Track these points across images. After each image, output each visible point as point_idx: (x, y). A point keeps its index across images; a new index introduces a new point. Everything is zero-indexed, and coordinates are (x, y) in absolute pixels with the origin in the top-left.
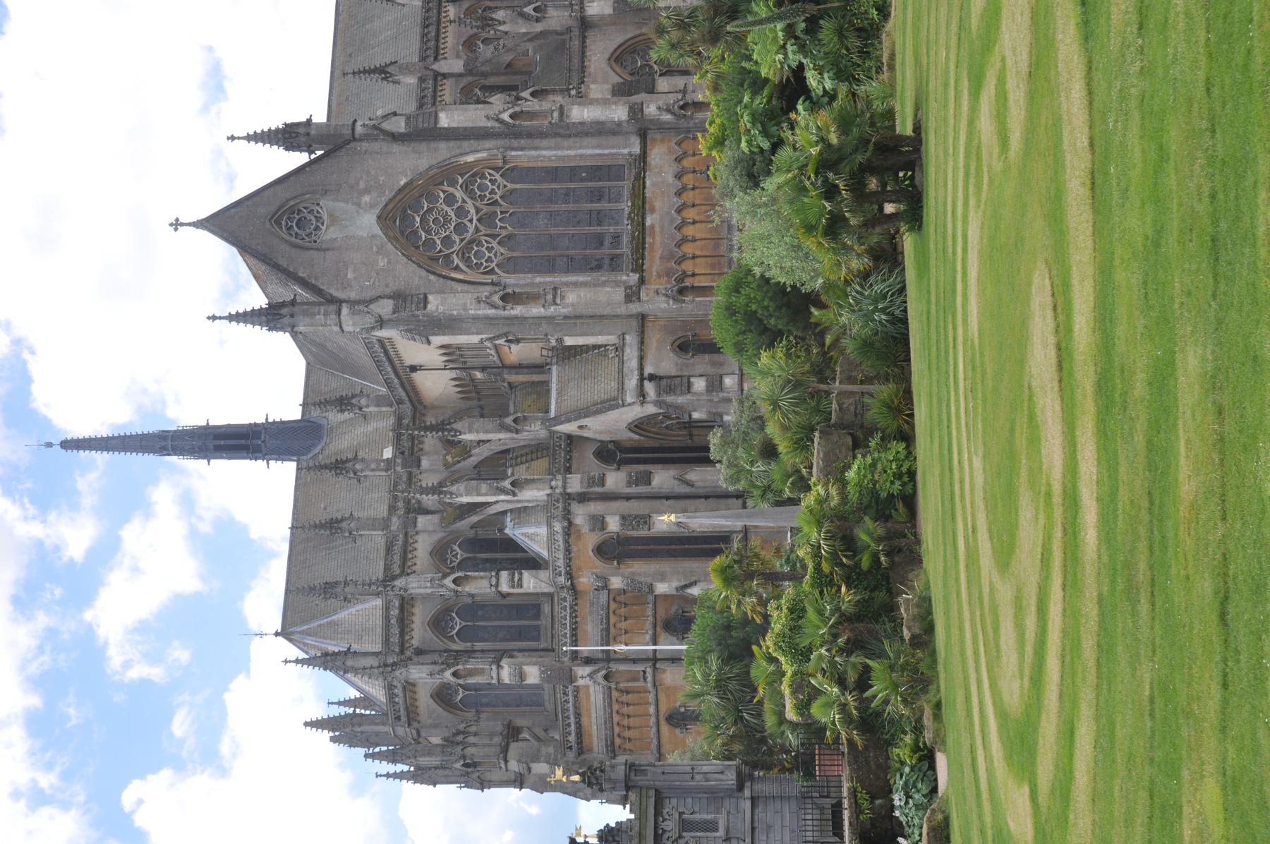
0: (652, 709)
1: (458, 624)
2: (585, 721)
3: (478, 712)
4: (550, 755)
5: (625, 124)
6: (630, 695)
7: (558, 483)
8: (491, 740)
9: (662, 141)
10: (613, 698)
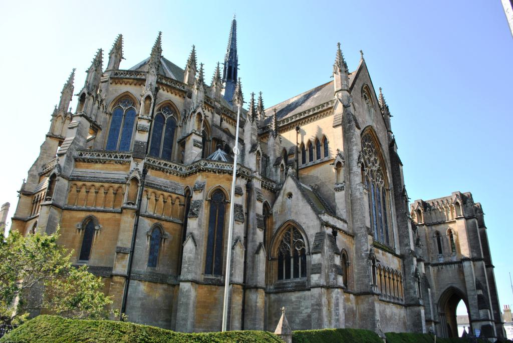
0: (99, 208)
1: (167, 117)
2: (99, 166)
3: (110, 114)
4: (79, 142)
5: (407, 248)
6: (113, 195)
7: (257, 175)
8: (94, 115)
9: (400, 265)
10: (113, 185)
